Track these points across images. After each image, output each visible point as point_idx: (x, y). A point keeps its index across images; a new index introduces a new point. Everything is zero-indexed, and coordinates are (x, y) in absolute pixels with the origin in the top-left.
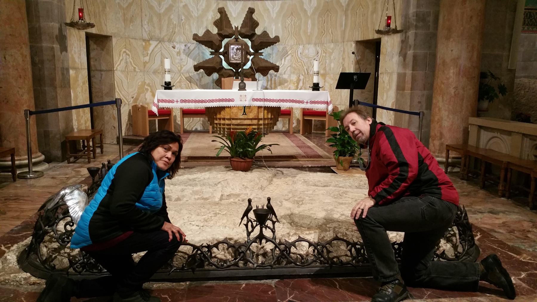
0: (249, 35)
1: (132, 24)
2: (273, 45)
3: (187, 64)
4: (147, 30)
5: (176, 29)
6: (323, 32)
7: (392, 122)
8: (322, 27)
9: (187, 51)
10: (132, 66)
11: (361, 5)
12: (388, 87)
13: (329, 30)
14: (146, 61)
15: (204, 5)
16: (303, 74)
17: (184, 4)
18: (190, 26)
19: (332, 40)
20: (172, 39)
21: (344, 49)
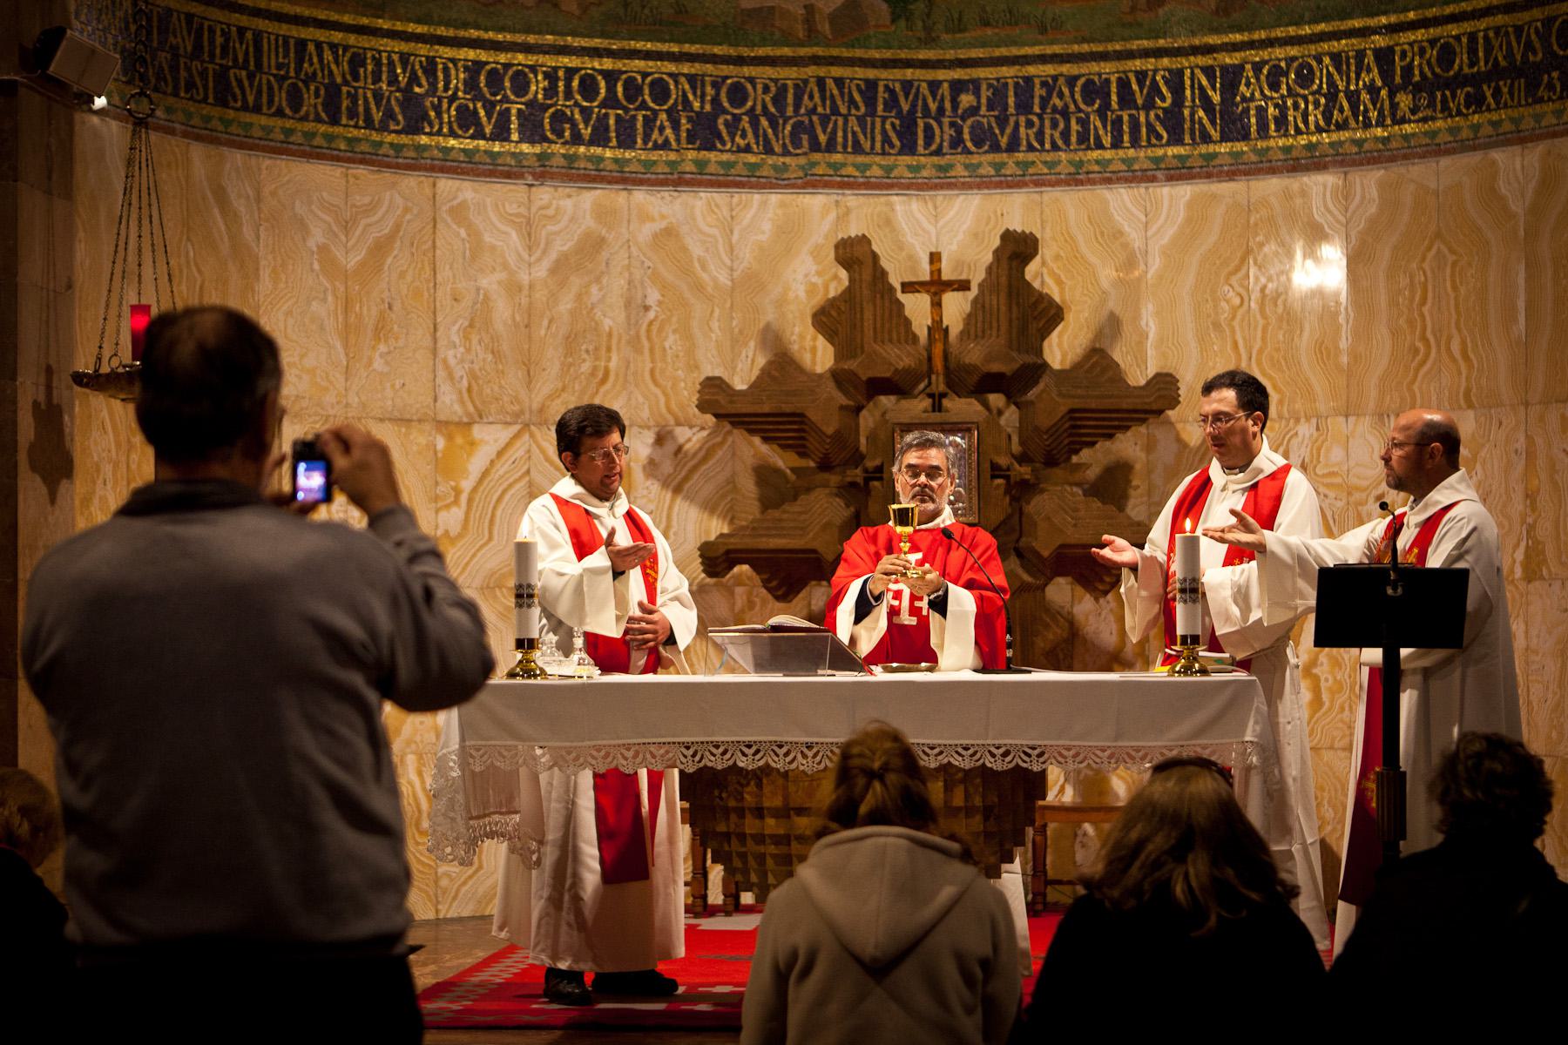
1: (382, 348)
2: (1143, 421)
4: (459, 372)
5: (615, 358)
8: (1411, 322)
9: (667, 467)
14: (447, 532)
15: (767, 226)
17: (659, 225)
18: (686, 333)
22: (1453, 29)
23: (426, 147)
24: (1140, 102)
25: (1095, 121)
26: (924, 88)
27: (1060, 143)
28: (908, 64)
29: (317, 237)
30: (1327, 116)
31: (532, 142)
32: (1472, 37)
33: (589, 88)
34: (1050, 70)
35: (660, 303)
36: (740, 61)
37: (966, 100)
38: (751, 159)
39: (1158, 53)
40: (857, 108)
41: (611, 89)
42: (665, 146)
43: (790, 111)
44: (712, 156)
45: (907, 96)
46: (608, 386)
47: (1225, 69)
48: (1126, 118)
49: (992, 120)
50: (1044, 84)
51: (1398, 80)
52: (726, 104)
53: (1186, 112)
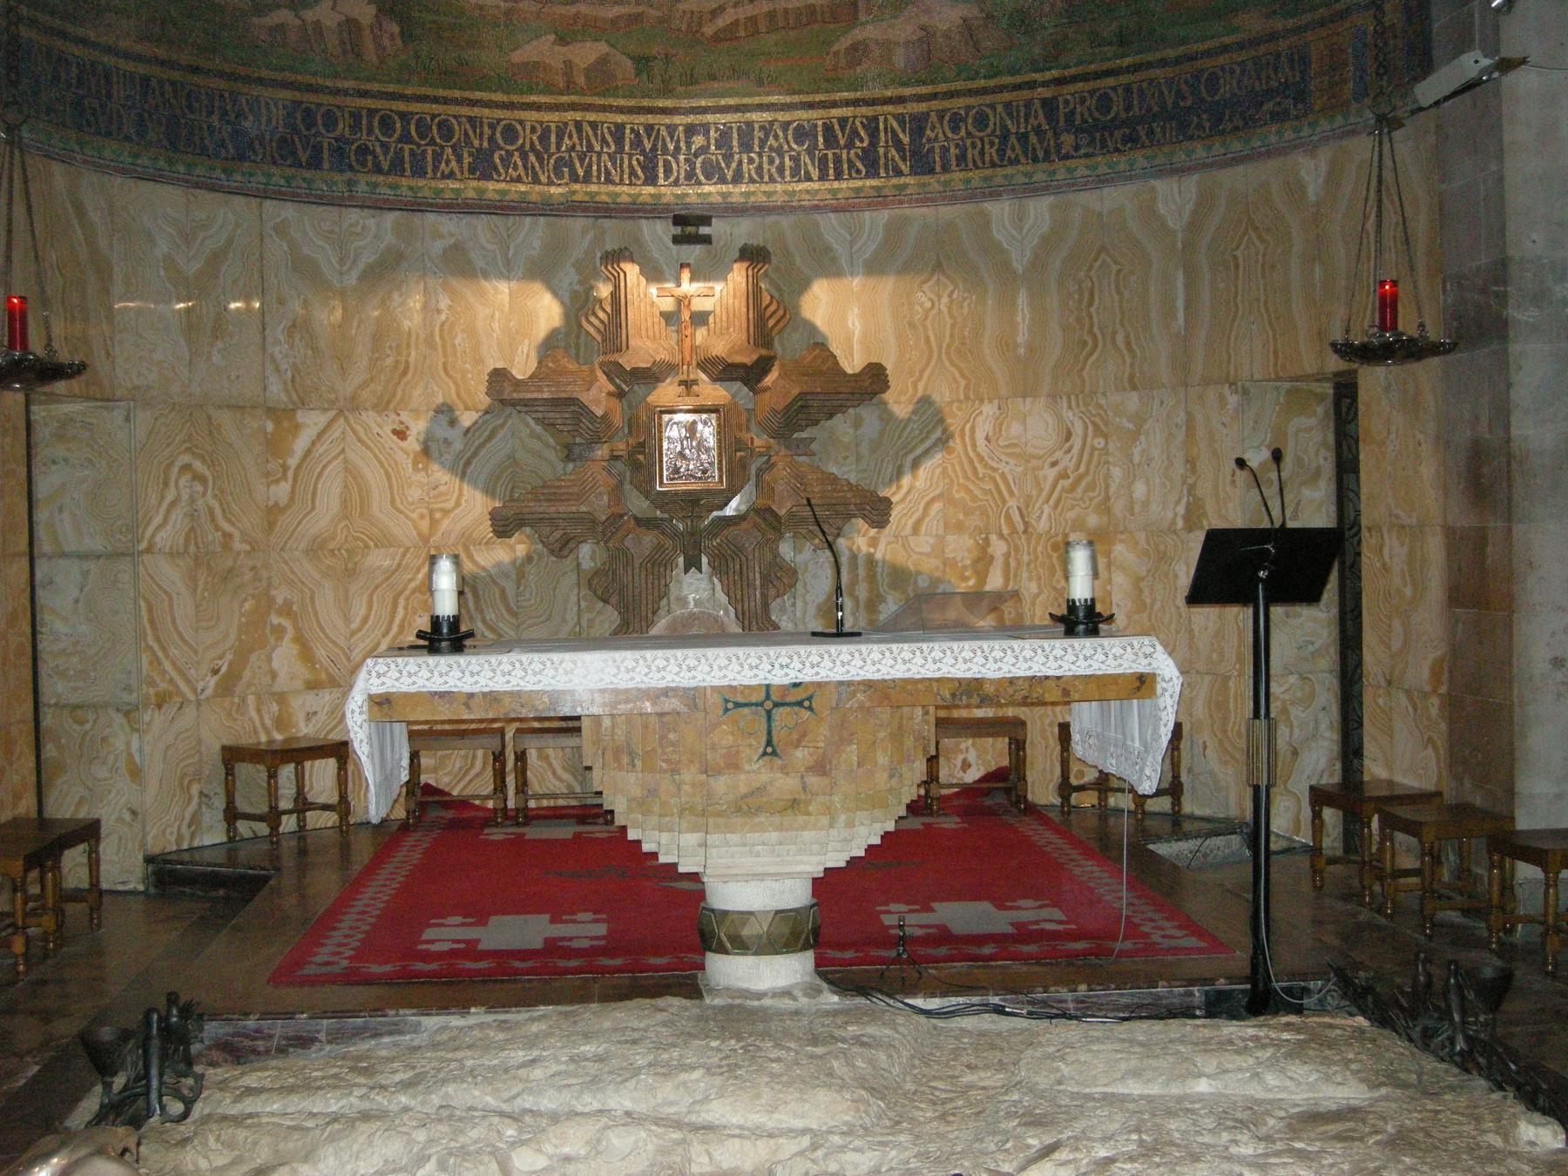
0: (743, 365)
1: (220, 344)
3: (458, 504)
4: (283, 367)
5: (413, 354)
6: (1085, 343)
7: (1442, 752)
8: (1079, 320)
10: (217, 528)
11: (1255, 229)
12: (1408, 591)
13: (1115, 333)
14: (276, 504)
15: (537, 244)
16: (1005, 531)
19: (1132, 377)
20: (394, 395)
21: (1190, 417)
22: (1111, 81)
24: (842, 142)
25: (805, 158)
26: (664, 132)
27: (776, 175)
28: (650, 111)
29: (163, 247)
30: (1001, 152)
31: (341, 171)
32: (1128, 89)
33: (387, 125)
34: (766, 116)
35: (450, 308)
36: (511, 106)
37: (699, 141)
38: (522, 188)
39: (855, 103)
40: (608, 146)
41: (405, 129)
42: (451, 175)
43: (553, 148)
44: (491, 185)
45: (649, 137)
46: (409, 376)
47: (913, 118)
48: (830, 156)
49: (720, 157)
50: (762, 128)
51: (1062, 123)
52: (500, 141)
53: (881, 151)
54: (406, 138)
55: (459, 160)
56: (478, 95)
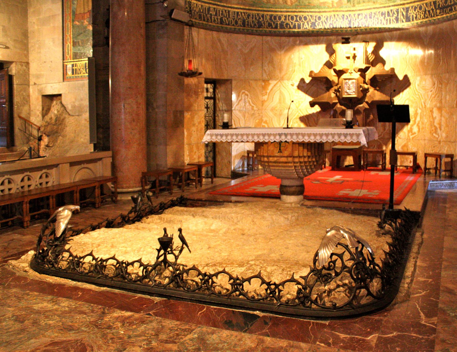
10: (250, 105)
23: (262, 31)
36: (320, 12)
41: (296, 19)
54: (297, 21)
55: (308, 24)
56: (312, 10)
